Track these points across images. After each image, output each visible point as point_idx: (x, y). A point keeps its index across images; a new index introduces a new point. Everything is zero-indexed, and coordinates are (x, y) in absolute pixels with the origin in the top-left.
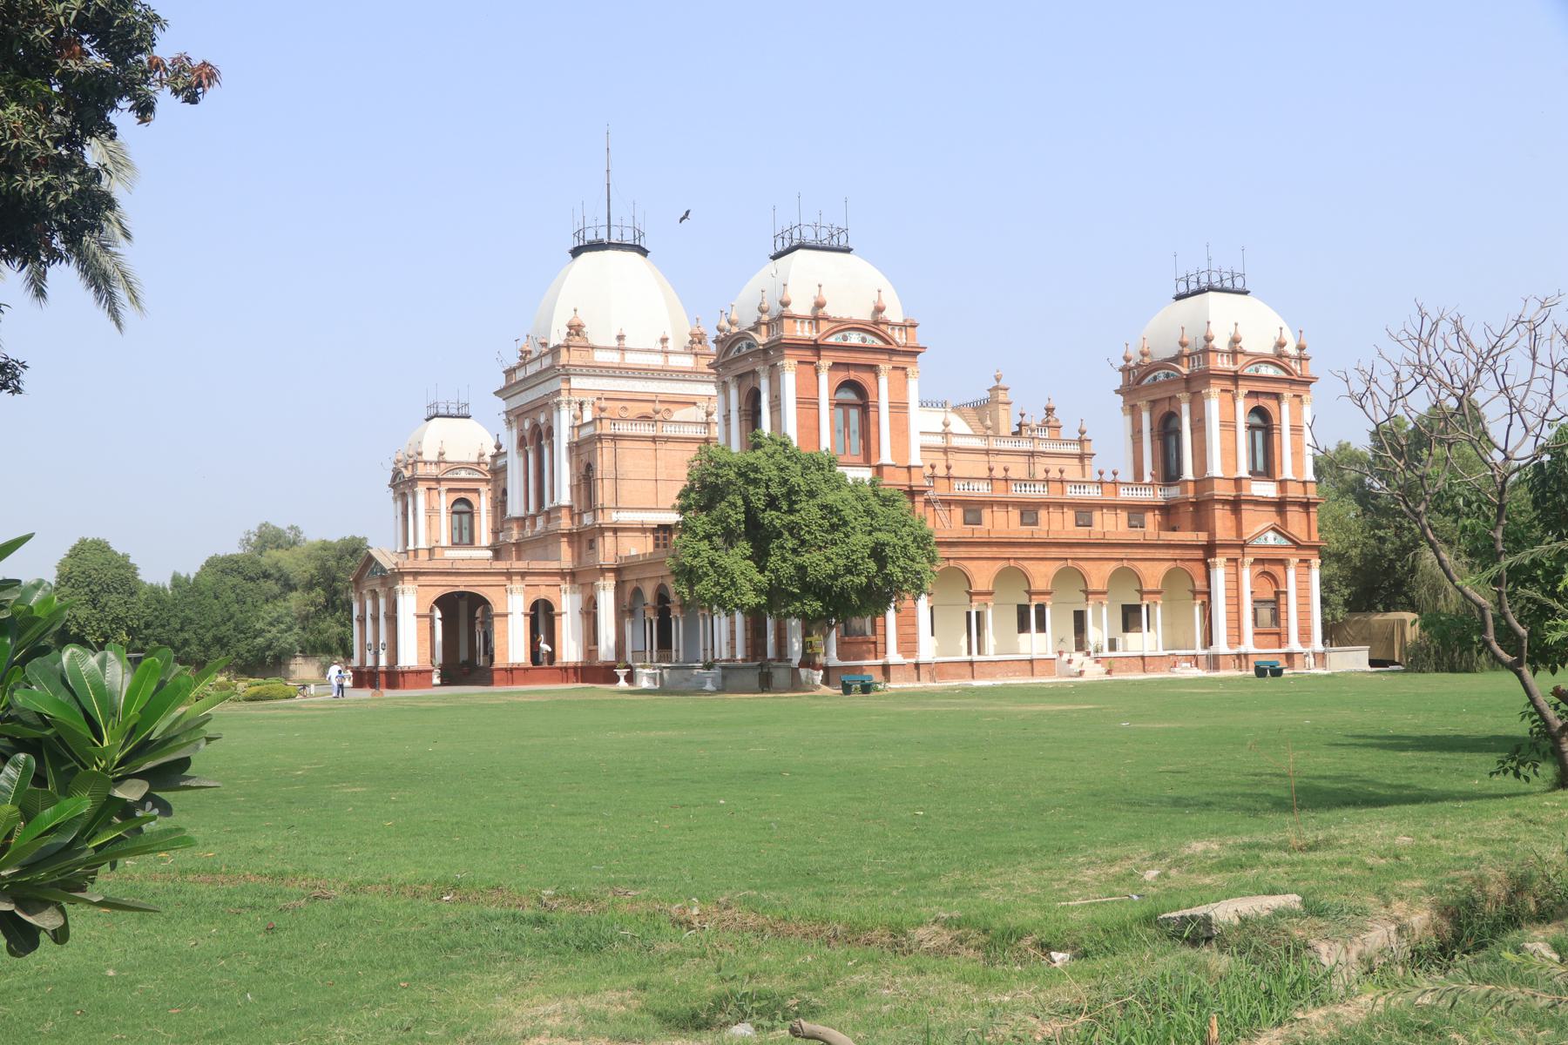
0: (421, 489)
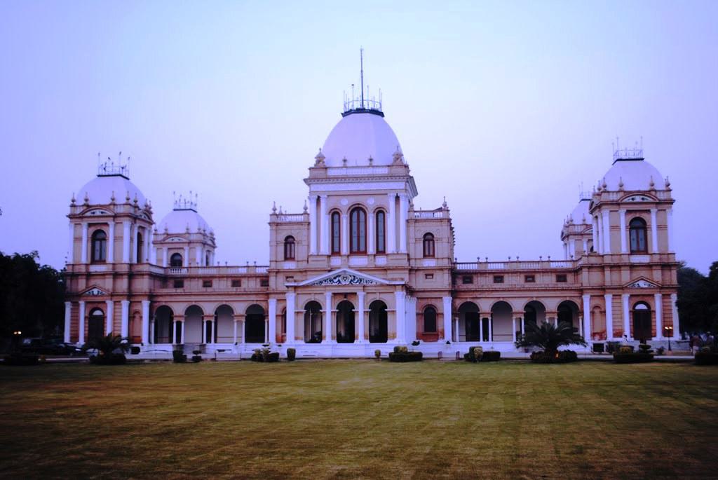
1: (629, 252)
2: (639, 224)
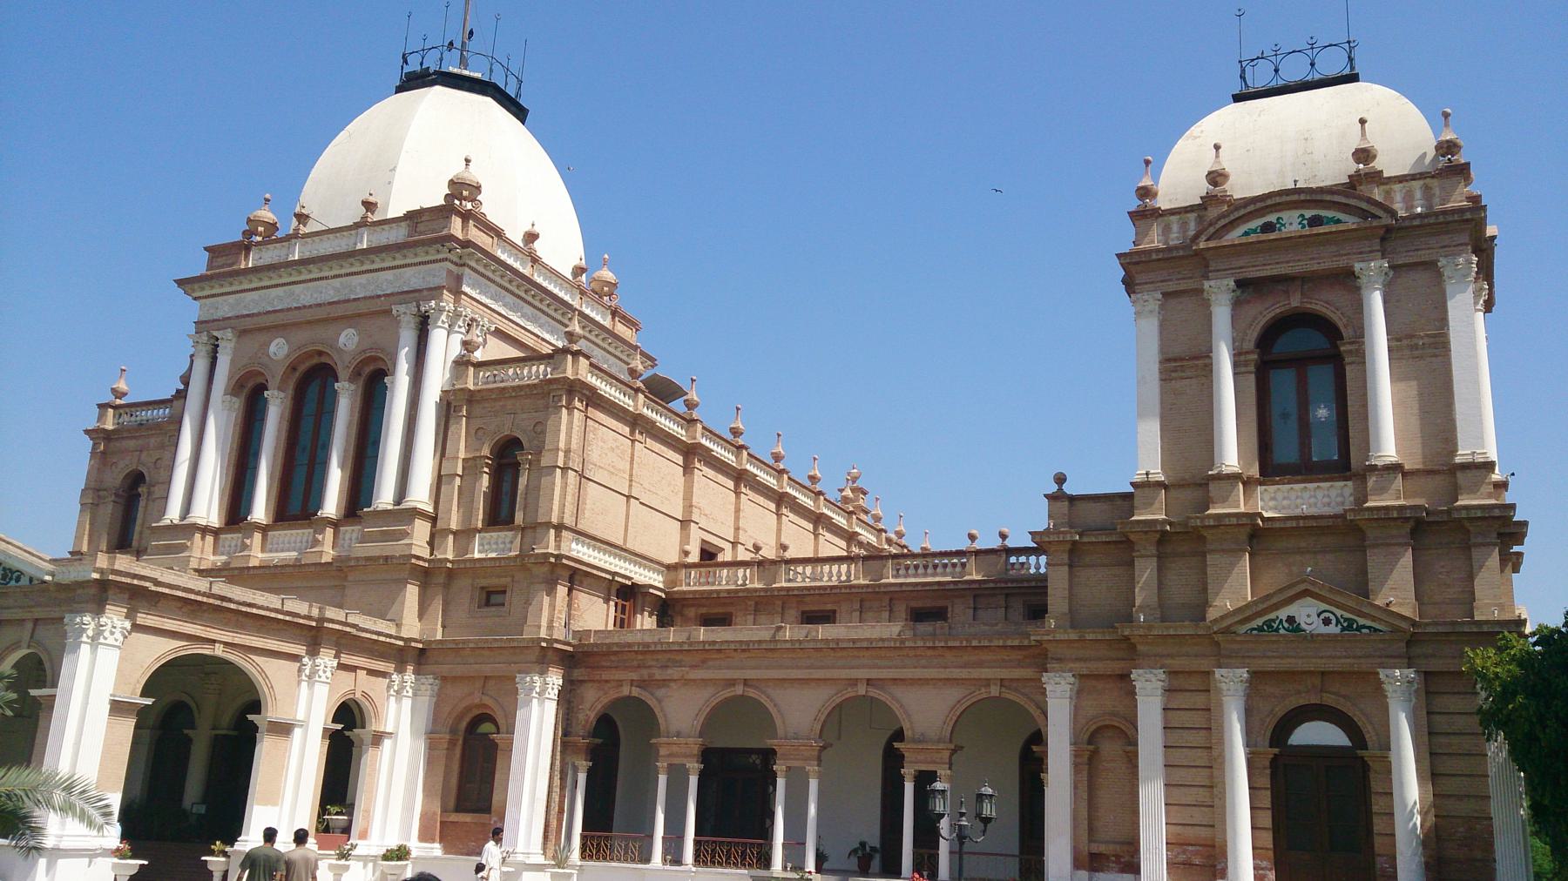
1: (1254, 471)
2: (1315, 341)
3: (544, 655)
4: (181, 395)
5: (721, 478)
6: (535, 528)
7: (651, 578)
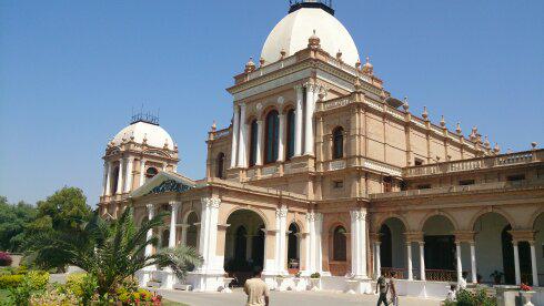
0: (131, 158)
3: (360, 204)
4: (232, 126)
5: (421, 134)
6: (351, 158)
7: (397, 173)
